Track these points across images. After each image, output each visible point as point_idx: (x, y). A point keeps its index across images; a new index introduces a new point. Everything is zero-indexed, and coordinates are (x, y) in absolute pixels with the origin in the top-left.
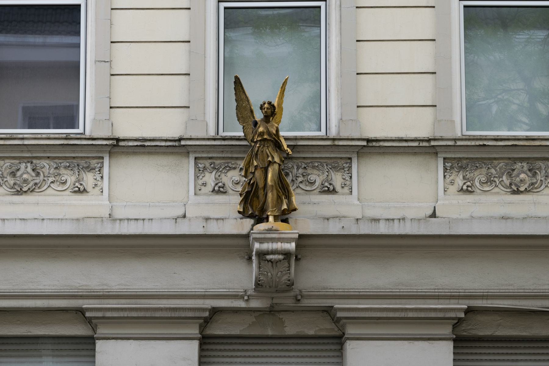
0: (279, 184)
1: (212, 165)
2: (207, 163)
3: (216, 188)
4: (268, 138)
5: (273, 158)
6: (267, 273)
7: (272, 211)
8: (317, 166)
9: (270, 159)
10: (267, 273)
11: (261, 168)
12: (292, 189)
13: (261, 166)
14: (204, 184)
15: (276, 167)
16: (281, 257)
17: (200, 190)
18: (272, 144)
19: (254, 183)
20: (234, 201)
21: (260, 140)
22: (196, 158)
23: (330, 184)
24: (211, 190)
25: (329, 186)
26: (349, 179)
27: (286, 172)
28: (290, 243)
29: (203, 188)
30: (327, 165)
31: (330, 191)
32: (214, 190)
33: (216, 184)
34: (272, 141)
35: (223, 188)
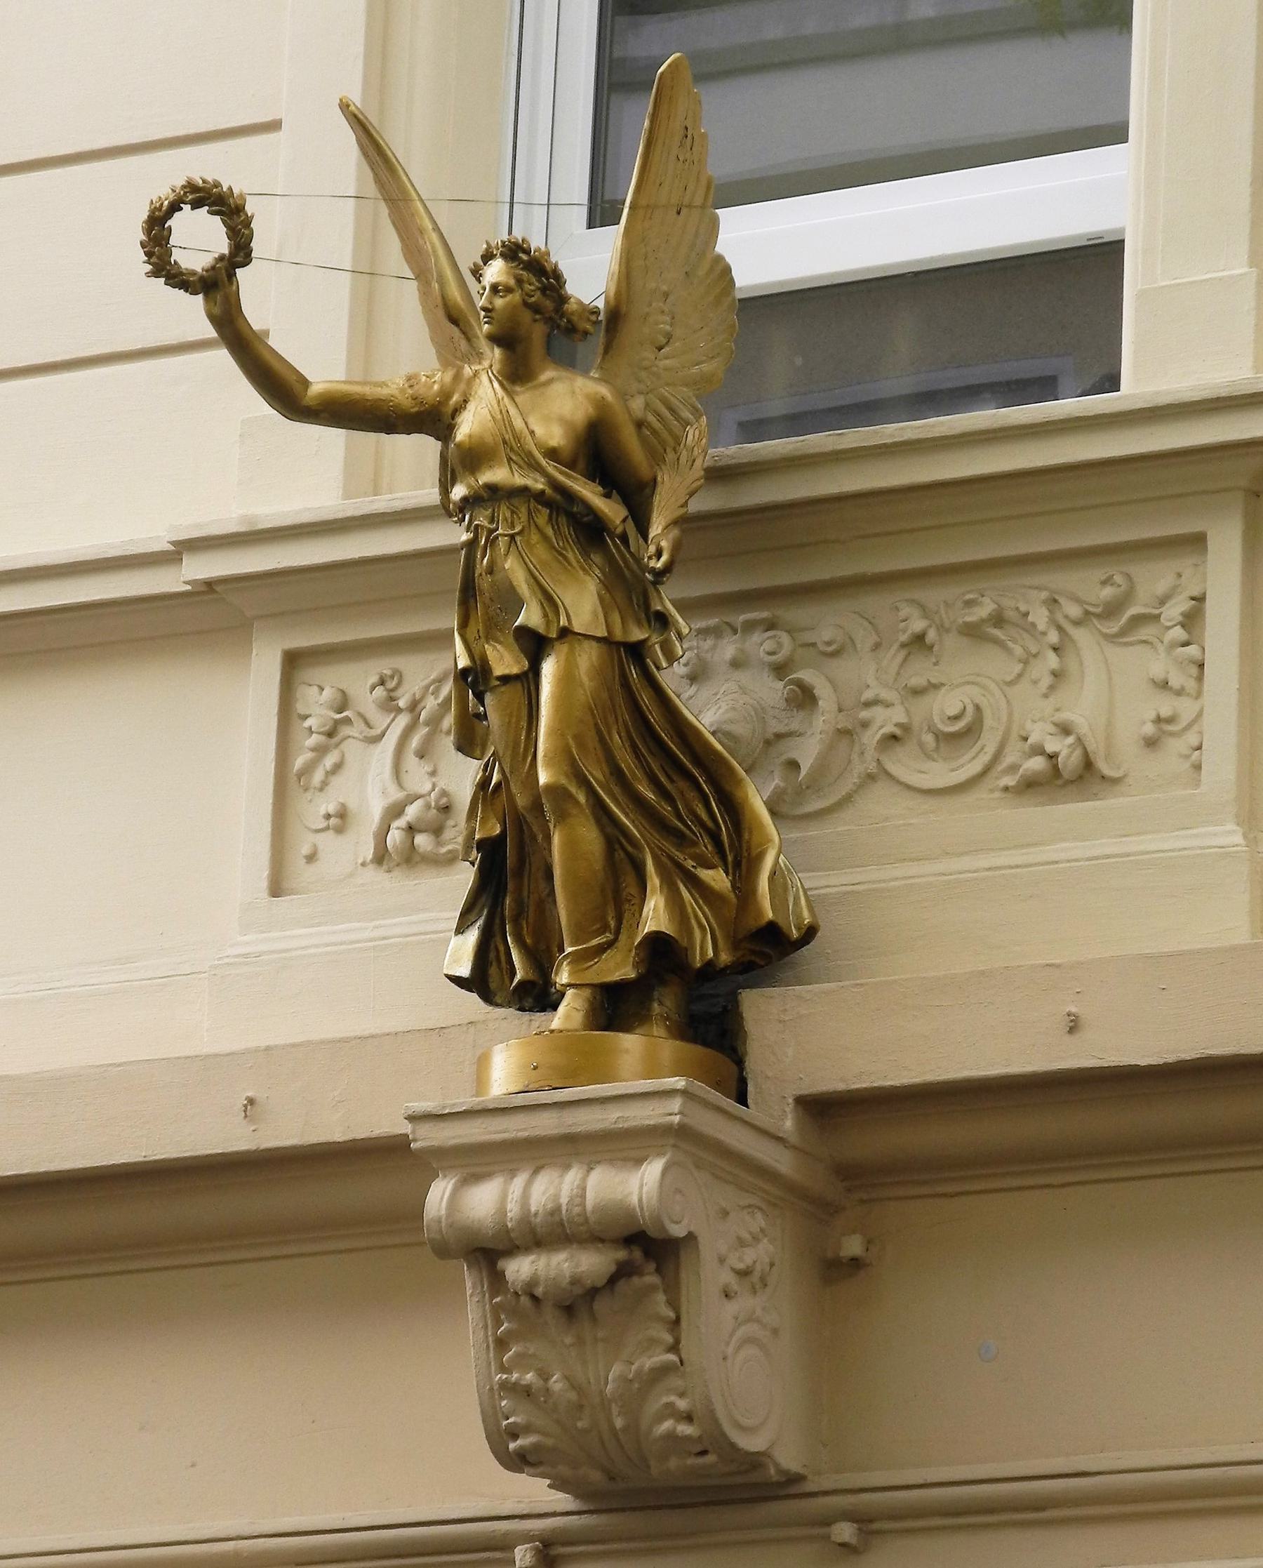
0: (617, 774)
1: (380, 691)
2: (359, 680)
3: (395, 837)
4: (519, 480)
5: (550, 602)
6: (545, 1376)
7: (578, 958)
8: (998, 620)
9: (530, 616)
10: (545, 1376)
11: (505, 679)
12: (756, 800)
13: (498, 671)
14: (341, 819)
15: (587, 658)
16: (590, 1263)
17: (311, 858)
18: (542, 516)
19: (498, 785)
20: (434, 921)
21: (465, 500)
22: (293, 661)
23: (1065, 729)
24: (370, 855)
25: (1050, 748)
26: (1191, 685)
27: (800, 684)
28: (639, 1162)
29: (328, 842)
30: (1053, 603)
31: (1074, 776)
32: (381, 856)
33: (395, 811)
34: (539, 497)
35: (437, 831)
